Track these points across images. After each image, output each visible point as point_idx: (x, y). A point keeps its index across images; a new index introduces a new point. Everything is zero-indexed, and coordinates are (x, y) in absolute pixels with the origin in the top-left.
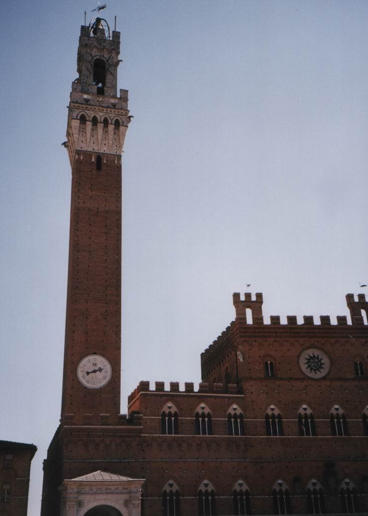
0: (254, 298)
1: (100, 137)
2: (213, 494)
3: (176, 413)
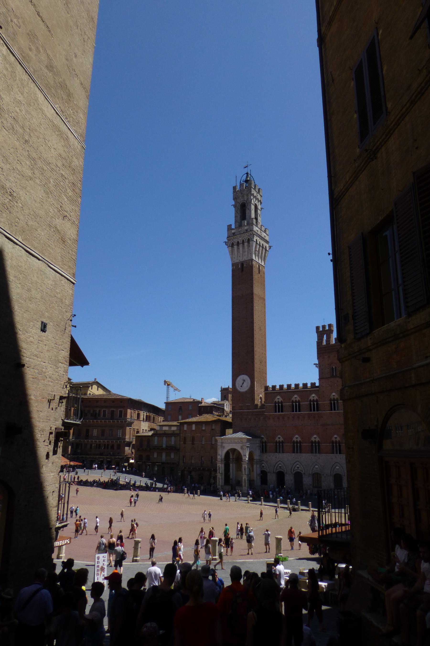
0: (327, 328)
1: (241, 252)
2: (300, 442)
3: (281, 401)
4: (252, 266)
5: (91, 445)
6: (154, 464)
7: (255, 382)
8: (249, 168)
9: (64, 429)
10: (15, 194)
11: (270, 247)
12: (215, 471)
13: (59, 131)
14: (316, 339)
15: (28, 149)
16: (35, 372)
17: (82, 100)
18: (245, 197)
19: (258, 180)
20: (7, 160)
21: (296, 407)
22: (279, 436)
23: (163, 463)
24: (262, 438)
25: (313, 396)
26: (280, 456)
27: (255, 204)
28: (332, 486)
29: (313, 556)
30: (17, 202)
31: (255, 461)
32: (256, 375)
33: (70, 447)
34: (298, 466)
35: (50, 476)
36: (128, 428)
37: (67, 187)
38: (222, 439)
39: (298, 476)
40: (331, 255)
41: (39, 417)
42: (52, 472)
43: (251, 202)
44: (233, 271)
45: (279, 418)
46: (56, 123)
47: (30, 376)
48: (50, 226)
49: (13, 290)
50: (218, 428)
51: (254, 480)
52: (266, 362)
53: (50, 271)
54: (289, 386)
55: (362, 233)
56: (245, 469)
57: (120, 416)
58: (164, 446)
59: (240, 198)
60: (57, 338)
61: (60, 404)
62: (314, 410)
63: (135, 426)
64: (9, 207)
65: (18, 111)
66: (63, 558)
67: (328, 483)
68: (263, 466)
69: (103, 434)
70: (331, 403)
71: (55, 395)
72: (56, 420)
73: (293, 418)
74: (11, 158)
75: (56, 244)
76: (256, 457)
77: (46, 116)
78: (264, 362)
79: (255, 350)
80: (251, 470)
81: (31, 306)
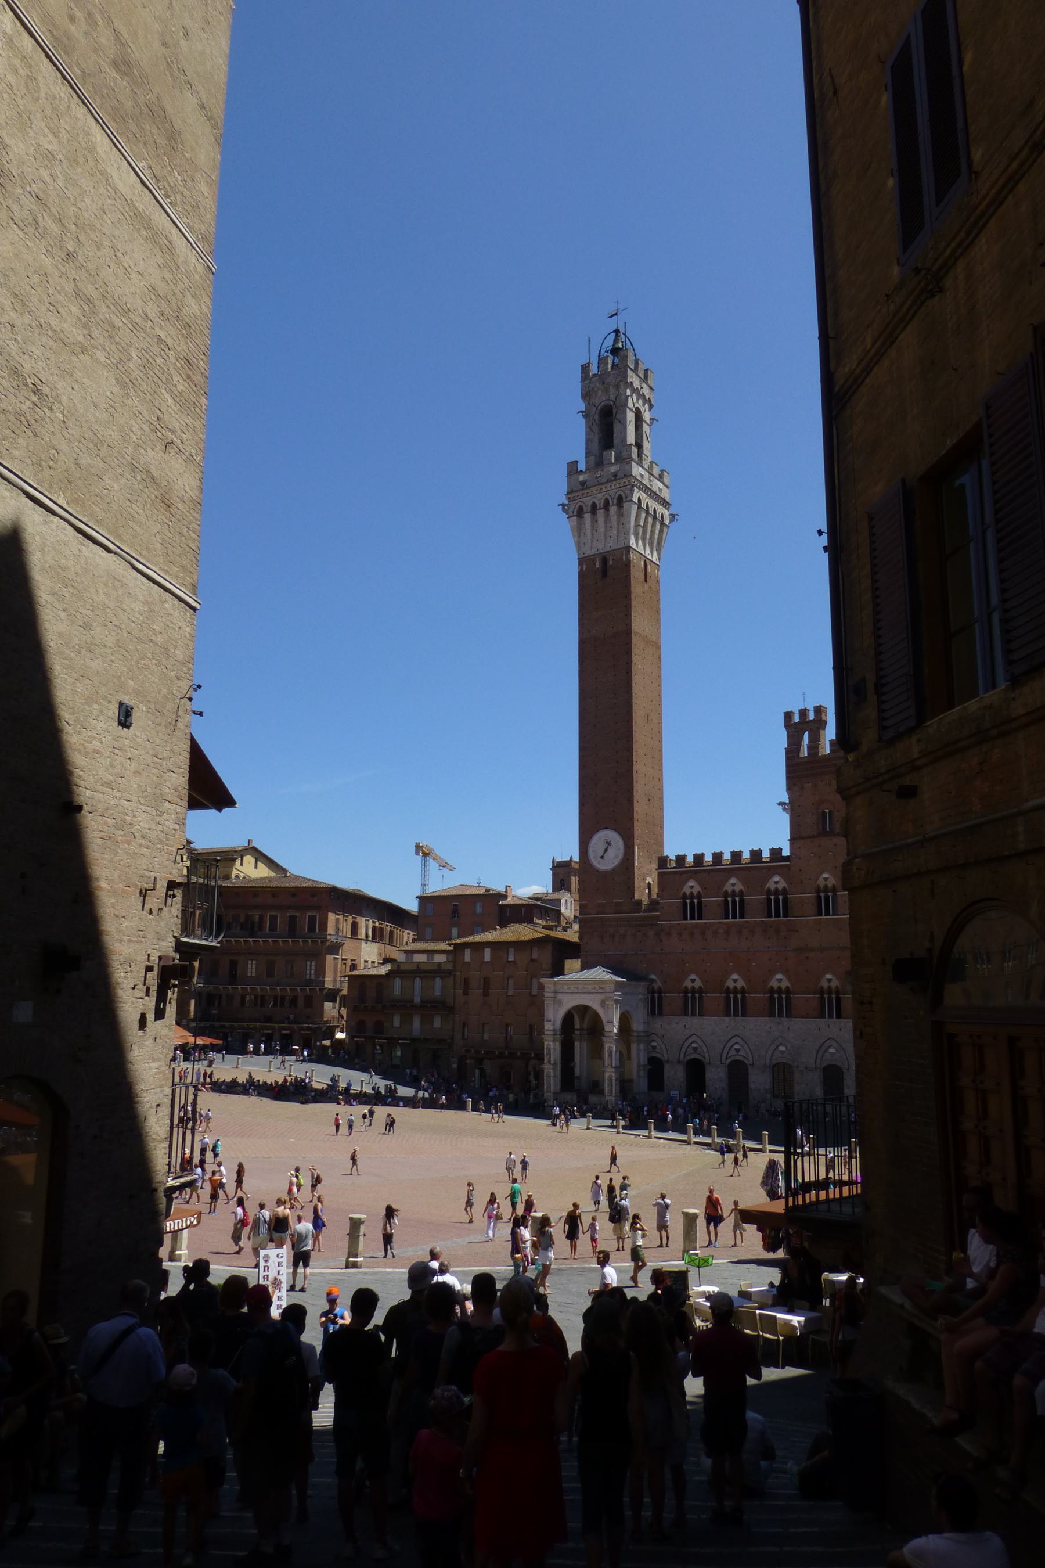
0: (811, 716)
1: (602, 530)
2: (743, 991)
4: (627, 565)
5: (243, 998)
6: (392, 1042)
7: (636, 848)
8: (622, 316)
9: (180, 960)
10: (46, 390)
11: (673, 517)
12: (540, 1057)
13: (150, 228)
14: (784, 743)
15: (73, 274)
16: (106, 823)
17: (204, 150)
18: (612, 390)
19: (644, 348)
20: (24, 304)
21: (735, 907)
22: (693, 976)
23: (414, 1040)
24: (653, 981)
25: (777, 882)
26: (694, 1023)
27: (637, 409)
28: (819, 1092)
29: (771, 1256)
30: (51, 409)
31: (635, 1034)
32: (638, 830)
33: (193, 1002)
34: (737, 1047)
35: (150, 1068)
36: (329, 958)
37: (172, 371)
38: (555, 983)
39: (738, 1071)
40: (825, 536)
41: (119, 931)
42: (154, 1060)
43: (625, 404)
44: (582, 576)
45: (692, 934)
46: (141, 207)
47: (96, 834)
48: (134, 468)
49: (48, 626)
50: (545, 957)
51: (631, 1081)
52: (661, 799)
53: (136, 579)
54: (717, 857)
55: (903, 481)
56: (610, 1055)
57: (312, 929)
58: (417, 1000)
59: (600, 393)
60: (158, 741)
61: (169, 901)
62: (778, 915)
63: (347, 952)
64: (33, 422)
65: (48, 179)
66: (183, 1259)
67: (808, 1086)
68: (654, 1048)
69: (270, 973)
70: (819, 898)
71: (155, 879)
72: (160, 938)
73: (728, 932)
74: (35, 299)
75: (149, 513)
76: (637, 1026)
77: (116, 190)
78: (656, 800)
79: (635, 769)
80: (624, 1057)
81: (93, 665)
